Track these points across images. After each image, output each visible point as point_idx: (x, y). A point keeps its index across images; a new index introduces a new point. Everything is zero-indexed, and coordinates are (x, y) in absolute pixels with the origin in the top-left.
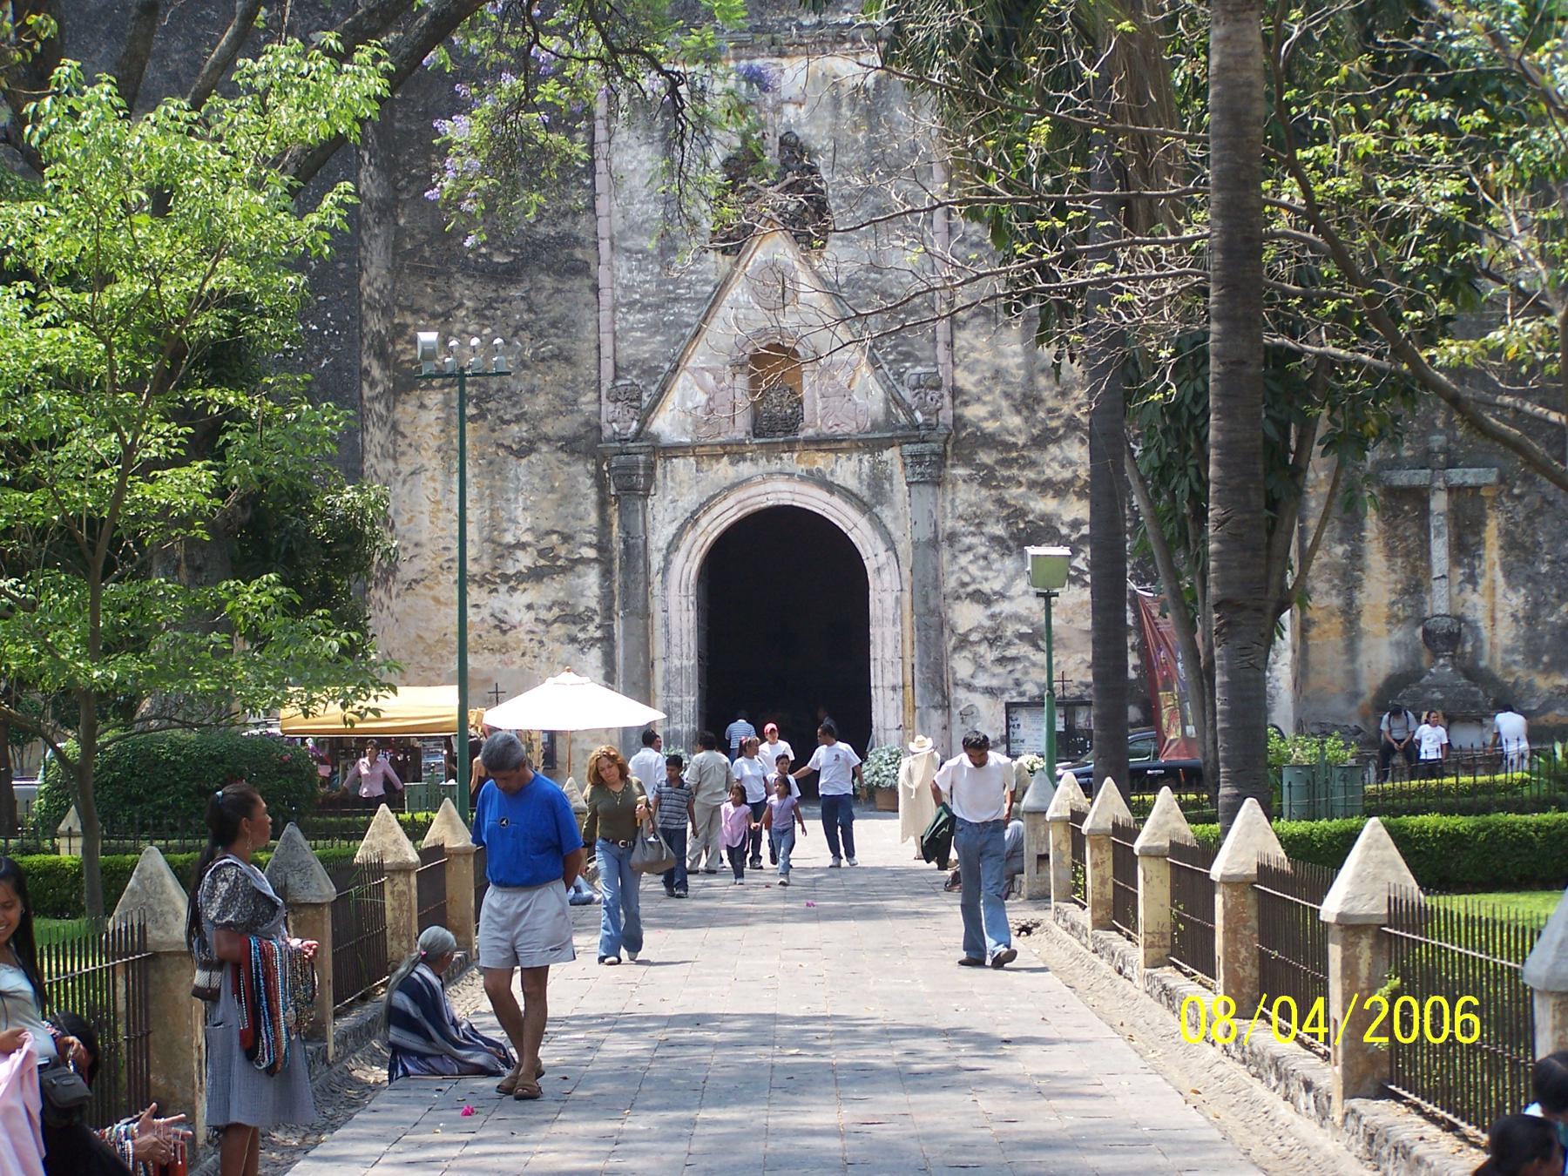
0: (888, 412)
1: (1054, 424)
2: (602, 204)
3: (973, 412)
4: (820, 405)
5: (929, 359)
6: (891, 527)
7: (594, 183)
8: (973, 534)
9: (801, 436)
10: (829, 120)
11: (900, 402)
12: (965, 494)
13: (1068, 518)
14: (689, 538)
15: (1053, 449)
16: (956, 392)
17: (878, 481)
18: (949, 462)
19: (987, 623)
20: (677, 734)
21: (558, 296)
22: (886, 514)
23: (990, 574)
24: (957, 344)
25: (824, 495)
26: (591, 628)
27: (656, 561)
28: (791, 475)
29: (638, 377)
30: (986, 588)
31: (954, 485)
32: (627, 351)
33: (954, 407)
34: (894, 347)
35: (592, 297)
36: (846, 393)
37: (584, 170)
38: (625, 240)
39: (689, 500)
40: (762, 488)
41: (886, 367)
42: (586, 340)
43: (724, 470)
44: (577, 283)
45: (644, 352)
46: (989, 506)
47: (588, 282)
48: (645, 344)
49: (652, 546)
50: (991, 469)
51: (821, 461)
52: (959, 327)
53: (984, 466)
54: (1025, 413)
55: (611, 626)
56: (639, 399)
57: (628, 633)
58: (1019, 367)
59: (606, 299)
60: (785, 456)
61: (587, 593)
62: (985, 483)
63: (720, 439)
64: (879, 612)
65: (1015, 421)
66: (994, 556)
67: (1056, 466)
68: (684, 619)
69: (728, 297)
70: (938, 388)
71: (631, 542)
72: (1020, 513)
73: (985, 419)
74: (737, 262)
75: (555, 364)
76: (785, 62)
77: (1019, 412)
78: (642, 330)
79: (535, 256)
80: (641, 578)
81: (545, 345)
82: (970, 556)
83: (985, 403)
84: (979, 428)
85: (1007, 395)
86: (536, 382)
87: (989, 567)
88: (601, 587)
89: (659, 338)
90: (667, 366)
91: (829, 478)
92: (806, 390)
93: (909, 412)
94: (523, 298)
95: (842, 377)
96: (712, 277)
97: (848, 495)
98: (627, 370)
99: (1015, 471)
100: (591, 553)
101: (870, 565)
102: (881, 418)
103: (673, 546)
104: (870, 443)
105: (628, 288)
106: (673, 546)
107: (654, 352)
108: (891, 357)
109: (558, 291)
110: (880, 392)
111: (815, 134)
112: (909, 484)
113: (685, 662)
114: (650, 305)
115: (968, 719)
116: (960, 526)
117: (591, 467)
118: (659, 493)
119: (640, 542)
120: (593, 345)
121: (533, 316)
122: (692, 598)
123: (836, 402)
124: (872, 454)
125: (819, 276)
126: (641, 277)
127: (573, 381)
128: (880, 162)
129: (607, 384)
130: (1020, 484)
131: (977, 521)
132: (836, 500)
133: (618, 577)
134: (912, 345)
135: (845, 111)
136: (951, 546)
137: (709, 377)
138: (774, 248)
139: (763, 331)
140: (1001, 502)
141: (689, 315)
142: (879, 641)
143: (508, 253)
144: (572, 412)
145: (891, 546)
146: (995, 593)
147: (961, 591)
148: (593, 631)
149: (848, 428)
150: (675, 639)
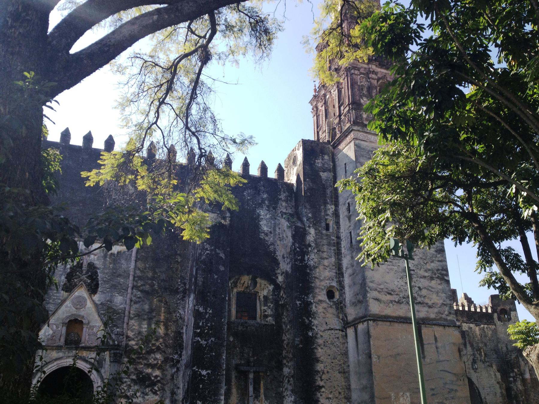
1: (153, 348)
3: (132, 343)
4: (87, 337)
6: (103, 374)
8: (127, 378)
9: (80, 345)
13: (154, 375)
15: (153, 355)
16: (128, 337)
22: (103, 371)
24: (130, 324)
40: (65, 360)
50: (134, 360)
53: (133, 358)
54: (146, 344)
58: (146, 331)
67: (152, 360)
69: (65, 304)
70: (123, 335)
72: (141, 373)
74: (70, 295)
84: (132, 348)
85: (141, 339)
92: (84, 333)
93: (114, 341)
96: (61, 298)
99: (141, 360)
112: (110, 362)
123: (92, 337)
125: (93, 301)
128: (115, 274)
130: (142, 364)
138: (81, 292)
139: (75, 315)
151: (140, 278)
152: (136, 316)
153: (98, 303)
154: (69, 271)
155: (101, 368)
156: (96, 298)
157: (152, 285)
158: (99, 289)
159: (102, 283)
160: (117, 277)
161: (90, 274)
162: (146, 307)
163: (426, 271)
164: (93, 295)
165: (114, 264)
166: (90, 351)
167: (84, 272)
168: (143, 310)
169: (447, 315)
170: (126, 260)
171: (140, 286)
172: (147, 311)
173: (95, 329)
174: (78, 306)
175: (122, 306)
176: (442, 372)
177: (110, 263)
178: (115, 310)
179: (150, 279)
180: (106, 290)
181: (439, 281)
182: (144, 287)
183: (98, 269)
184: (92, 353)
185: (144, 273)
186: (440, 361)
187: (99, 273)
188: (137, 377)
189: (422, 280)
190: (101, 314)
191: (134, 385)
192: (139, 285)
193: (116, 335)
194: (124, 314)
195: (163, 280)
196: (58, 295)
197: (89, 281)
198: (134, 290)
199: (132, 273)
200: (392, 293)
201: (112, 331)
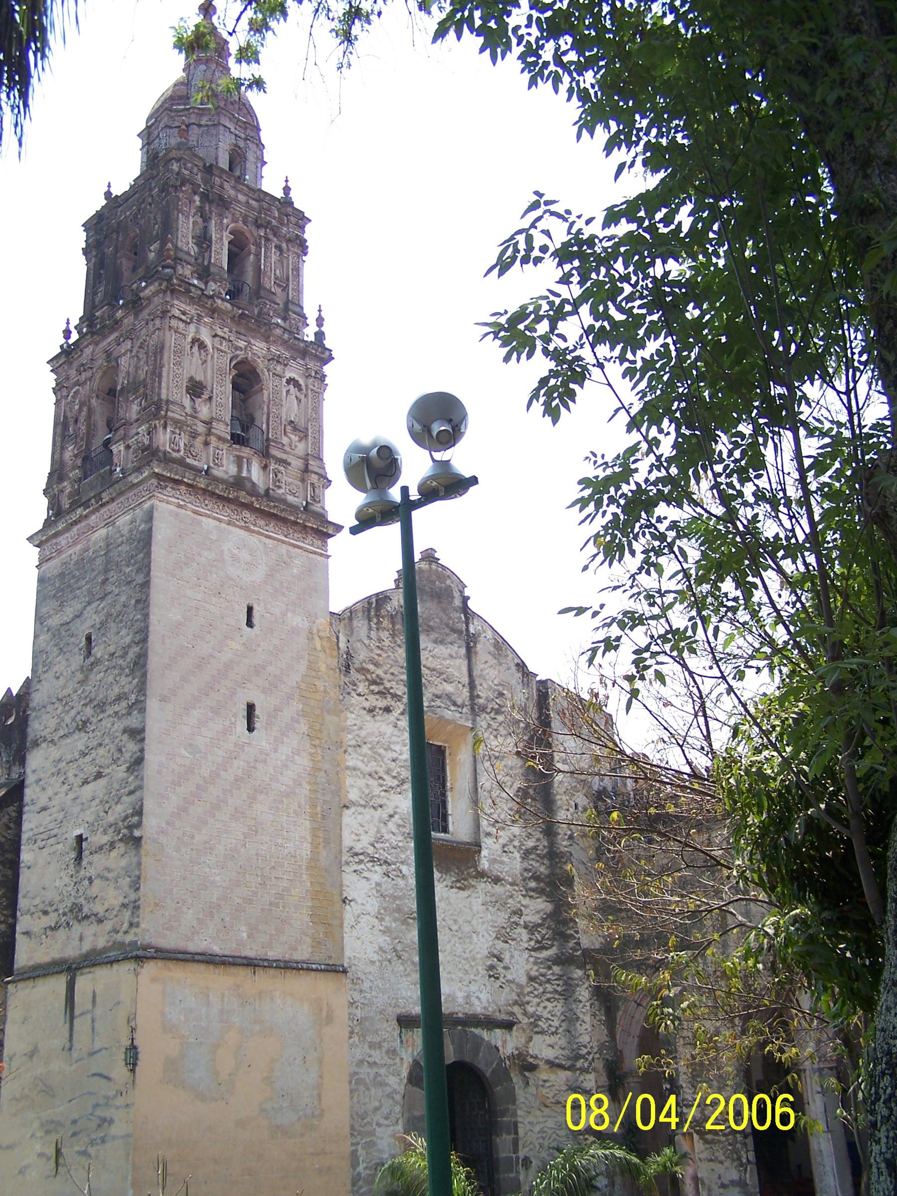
163: (105, 832)
169: (126, 932)
176: (96, 1078)
181: (121, 848)
186: (95, 1052)
189: (96, 856)
200: (49, 909)
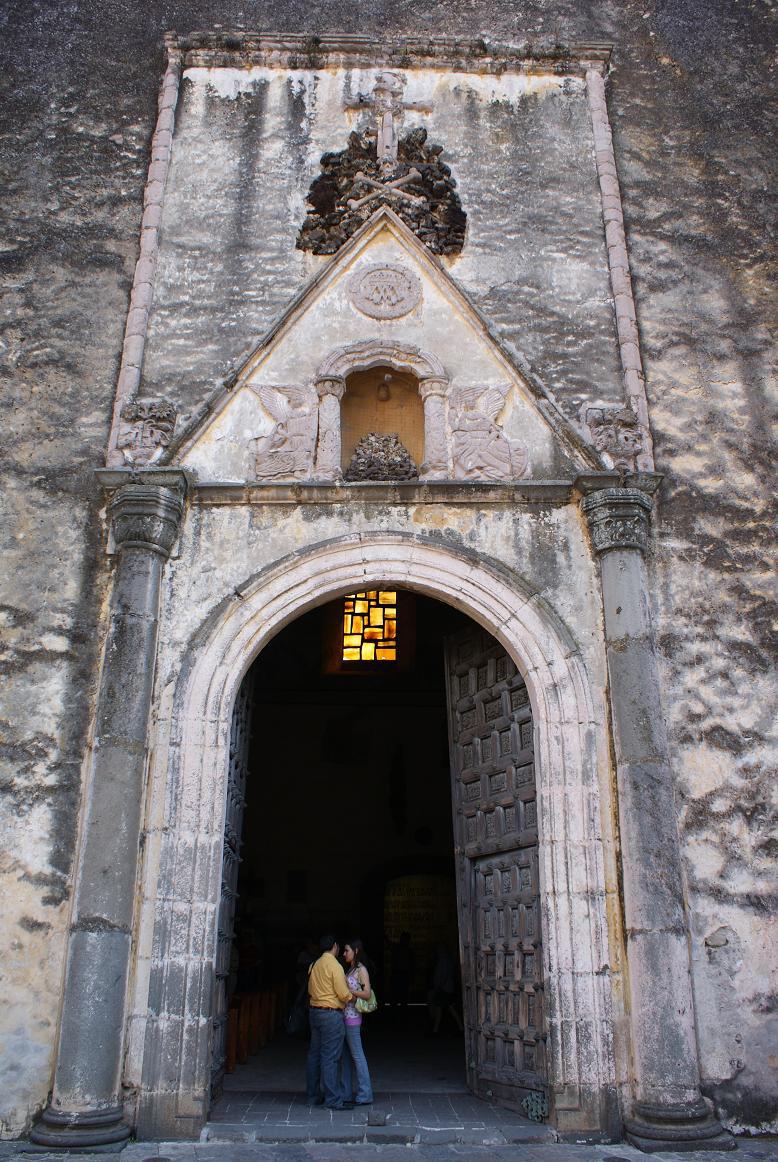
0: (557, 456)
2: (153, 193)
3: (682, 465)
5: (614, 392)
6: (571, 621)
7: (146, 174)
8: (703, 639)
10: (464, 128)
11: (574, 441)
12: (689, 580)
14: (226, 627)
16: (658, 438)
17: (545, 555)
18: (656, 530)
19: (739, 782)
20: (177, 974)
21: (73, 292)
22: (564, 602)
23: (736, 702)
24: (651, 377)
25: (461, 568)
26: (40, 768)
27: (168, 660)
28: (407, 535)
29: (172, 394)
30: (731, 723)
31: (666, 566)
32: (160, 362)
33: (655, 456)
34: (564, 373)
35: (121, 294)
36: (493, 429)
37: (135, 161)
38: (178, 235)
39: (233, 569)
40: (357, 555)
41: (552, 397)
42: (102, 345)
43: (295, 528)
44: (106, 278)
45: (187, 365)
46: (723, 597)
47: (118, 277)
48: (188, 354)
49: (161, 637)
50: (719, 545)
51: (454, 520)
52: (652, 357)
53: (705, 539)
54: (759, 469)
55: (77, 768)
56: (170, 418)
57: (103, 775)
58: (742, 411)
59: (140, 294)
60: (394, 510)
61: (44, 708)
62: (712, 562)
63: (290, 480)
64: (556, 758)
65: (746, 480)
66: (738, 673)
68: (208, 761)
69: (319, 302)
70: (630, 425)
71: (130, 621)
73: (702, 475)
74: (336, 261)
75: (51, 371)
76: (408, 73)
77: (750, 468)
78: (187, 337)
79: (49, 244)
80: (139, 682)
81: (42, 346)
82: (700, 672)
83: (699, 454)
84: (693, 487)
85: (730, 446)
86: (17, 393)
87: (732, 690)
88: (68, 699)
89: (211, 347)
90: (219, 382)
91: (467, 544)
93: (592, 454)
94: (21, 290)
95: (483, 406)
96: (296, 278)
97: (499, 569)
98: (158, 386)
99: (755, 548)
100: (60, 644)
101: (538, 683)
102: (547, 463)
103: (199, 638)
104: (537, 497)
105: (171, 289)
106: (199, 638)
107: (200, 365)
108: (558, 385)
109: (73, 284)
110: (545, 430)
111: (448, 137)
112: (598, 554)
113: (203, 838)
114: (205, 308)
115: (719, 954)
116: (680, 625)
117: (80, 513)
118: (186, 557)
119: (146, 625)
120: (111, 352)
121: (31, 313)
122: (225, 726)
123: (476, 439)
124: (536, 513)
125: (449, 278)
126: (196, 276)
127: (72, 395)
128: (526, 175)
129: (124, 397)
130: (765, 567)
131: (709, 621)
132: (479, 575)
133: (100, 682)
134: (588, 373)
135: (484, 122)
136: (669, 655)
137: (281, 401)
139: (372, 343)
140: (739, 591)
141: (259, 321)
142: (558, 810)
143: (12, 241)
144: (64, 435)
145: (575, 650)
146: (747, 733)
147: (691, 728)
148: (44, 775)
149: (499, 472)
150: (189, 797)
151: (648, 189)
152: (673, 344)
153: (483, 290)
154: (318, 173)
155: (555, 587)
156: (461, 267)
157: (717, 217)
158: (471, 235)
159: (476, 213)
160: (544, 186)
161: (414, 173)
162: (715, 303)
164: (443, 260)
165: (517, 141)
166: (478, 506)
167: (388, 170)
168: (703, 316)
170: (567, 122)
171: (658, 221)
172: (725, 319)
173: (481, 401)
174: (385, 308)
175: (595, 303)
177: (498, 138)
178: (563, 321)
179: (697, 192)
180: (502, 239)
182: (679, 223)
183: (449, 158)
184: (491, 514)
185: (664, 168)
187: (455, 175)
188: (757, 628)
190: (502, 334)
191: (753, 672)
192: (653, 214)
193: (598, 423)
194: (616, 334)
195: (757, 195)
196: (279, 267)
197: (417, 201)
198: (636, 237)
199: (607, 170)
201: (573, 410)
